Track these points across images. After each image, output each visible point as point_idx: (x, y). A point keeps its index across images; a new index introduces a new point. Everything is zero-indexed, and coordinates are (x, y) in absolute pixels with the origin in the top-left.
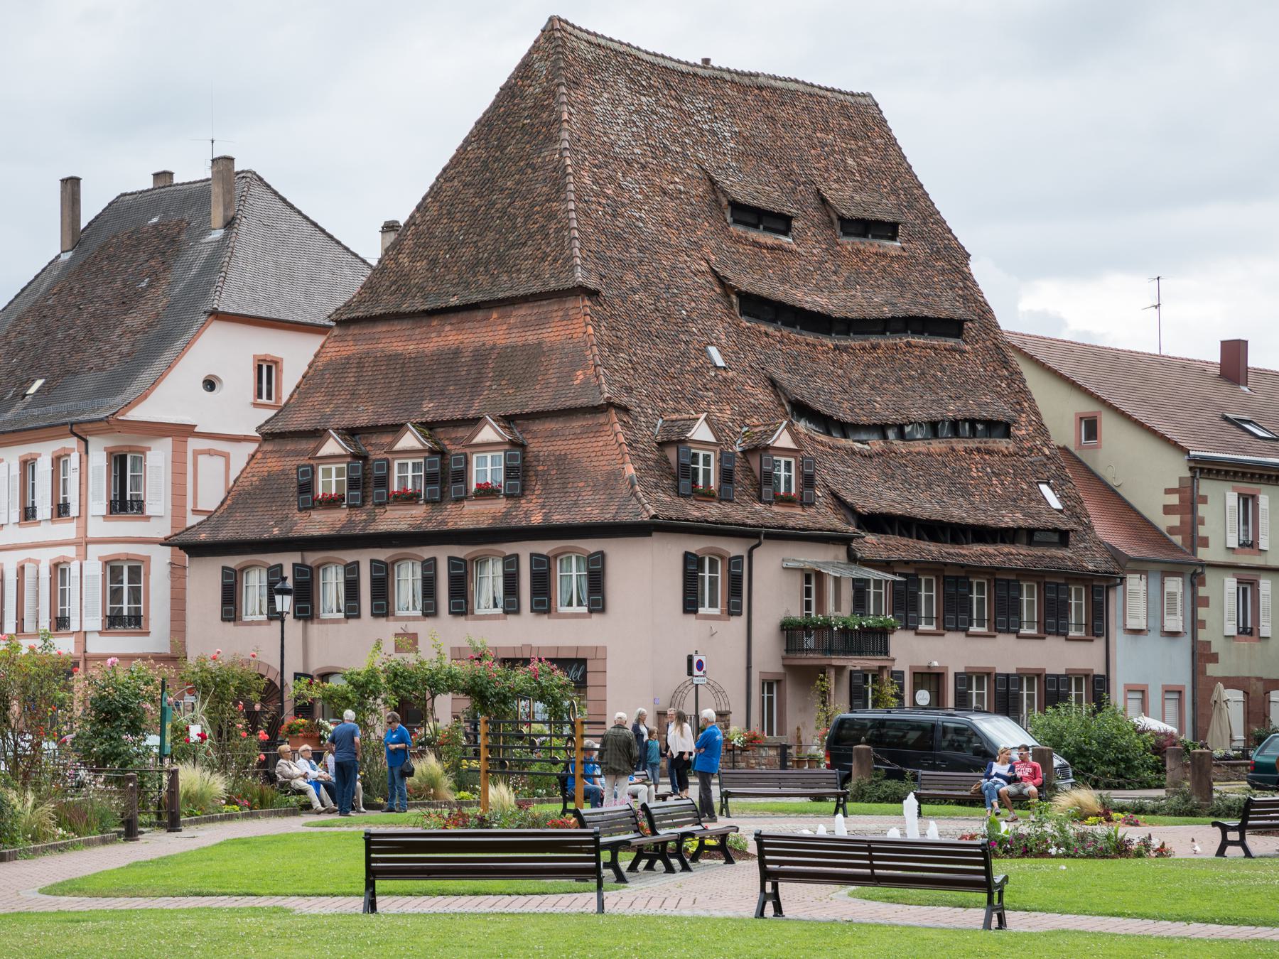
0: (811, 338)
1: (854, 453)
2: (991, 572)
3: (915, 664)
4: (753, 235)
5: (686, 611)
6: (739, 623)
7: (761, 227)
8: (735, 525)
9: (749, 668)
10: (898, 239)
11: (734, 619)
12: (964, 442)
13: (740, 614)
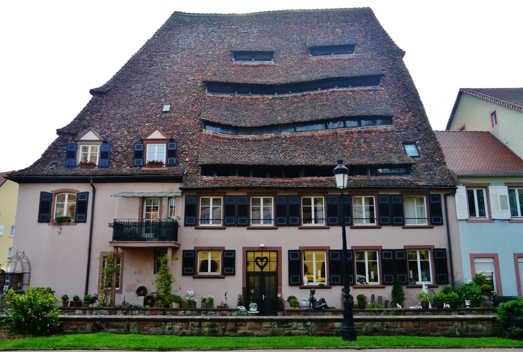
0: (258, 96)
1: (248, 140)
7: (253, 59)
9: (90, 250)
10: (354, 53)
11: (80, 225)
12: (347, 129)
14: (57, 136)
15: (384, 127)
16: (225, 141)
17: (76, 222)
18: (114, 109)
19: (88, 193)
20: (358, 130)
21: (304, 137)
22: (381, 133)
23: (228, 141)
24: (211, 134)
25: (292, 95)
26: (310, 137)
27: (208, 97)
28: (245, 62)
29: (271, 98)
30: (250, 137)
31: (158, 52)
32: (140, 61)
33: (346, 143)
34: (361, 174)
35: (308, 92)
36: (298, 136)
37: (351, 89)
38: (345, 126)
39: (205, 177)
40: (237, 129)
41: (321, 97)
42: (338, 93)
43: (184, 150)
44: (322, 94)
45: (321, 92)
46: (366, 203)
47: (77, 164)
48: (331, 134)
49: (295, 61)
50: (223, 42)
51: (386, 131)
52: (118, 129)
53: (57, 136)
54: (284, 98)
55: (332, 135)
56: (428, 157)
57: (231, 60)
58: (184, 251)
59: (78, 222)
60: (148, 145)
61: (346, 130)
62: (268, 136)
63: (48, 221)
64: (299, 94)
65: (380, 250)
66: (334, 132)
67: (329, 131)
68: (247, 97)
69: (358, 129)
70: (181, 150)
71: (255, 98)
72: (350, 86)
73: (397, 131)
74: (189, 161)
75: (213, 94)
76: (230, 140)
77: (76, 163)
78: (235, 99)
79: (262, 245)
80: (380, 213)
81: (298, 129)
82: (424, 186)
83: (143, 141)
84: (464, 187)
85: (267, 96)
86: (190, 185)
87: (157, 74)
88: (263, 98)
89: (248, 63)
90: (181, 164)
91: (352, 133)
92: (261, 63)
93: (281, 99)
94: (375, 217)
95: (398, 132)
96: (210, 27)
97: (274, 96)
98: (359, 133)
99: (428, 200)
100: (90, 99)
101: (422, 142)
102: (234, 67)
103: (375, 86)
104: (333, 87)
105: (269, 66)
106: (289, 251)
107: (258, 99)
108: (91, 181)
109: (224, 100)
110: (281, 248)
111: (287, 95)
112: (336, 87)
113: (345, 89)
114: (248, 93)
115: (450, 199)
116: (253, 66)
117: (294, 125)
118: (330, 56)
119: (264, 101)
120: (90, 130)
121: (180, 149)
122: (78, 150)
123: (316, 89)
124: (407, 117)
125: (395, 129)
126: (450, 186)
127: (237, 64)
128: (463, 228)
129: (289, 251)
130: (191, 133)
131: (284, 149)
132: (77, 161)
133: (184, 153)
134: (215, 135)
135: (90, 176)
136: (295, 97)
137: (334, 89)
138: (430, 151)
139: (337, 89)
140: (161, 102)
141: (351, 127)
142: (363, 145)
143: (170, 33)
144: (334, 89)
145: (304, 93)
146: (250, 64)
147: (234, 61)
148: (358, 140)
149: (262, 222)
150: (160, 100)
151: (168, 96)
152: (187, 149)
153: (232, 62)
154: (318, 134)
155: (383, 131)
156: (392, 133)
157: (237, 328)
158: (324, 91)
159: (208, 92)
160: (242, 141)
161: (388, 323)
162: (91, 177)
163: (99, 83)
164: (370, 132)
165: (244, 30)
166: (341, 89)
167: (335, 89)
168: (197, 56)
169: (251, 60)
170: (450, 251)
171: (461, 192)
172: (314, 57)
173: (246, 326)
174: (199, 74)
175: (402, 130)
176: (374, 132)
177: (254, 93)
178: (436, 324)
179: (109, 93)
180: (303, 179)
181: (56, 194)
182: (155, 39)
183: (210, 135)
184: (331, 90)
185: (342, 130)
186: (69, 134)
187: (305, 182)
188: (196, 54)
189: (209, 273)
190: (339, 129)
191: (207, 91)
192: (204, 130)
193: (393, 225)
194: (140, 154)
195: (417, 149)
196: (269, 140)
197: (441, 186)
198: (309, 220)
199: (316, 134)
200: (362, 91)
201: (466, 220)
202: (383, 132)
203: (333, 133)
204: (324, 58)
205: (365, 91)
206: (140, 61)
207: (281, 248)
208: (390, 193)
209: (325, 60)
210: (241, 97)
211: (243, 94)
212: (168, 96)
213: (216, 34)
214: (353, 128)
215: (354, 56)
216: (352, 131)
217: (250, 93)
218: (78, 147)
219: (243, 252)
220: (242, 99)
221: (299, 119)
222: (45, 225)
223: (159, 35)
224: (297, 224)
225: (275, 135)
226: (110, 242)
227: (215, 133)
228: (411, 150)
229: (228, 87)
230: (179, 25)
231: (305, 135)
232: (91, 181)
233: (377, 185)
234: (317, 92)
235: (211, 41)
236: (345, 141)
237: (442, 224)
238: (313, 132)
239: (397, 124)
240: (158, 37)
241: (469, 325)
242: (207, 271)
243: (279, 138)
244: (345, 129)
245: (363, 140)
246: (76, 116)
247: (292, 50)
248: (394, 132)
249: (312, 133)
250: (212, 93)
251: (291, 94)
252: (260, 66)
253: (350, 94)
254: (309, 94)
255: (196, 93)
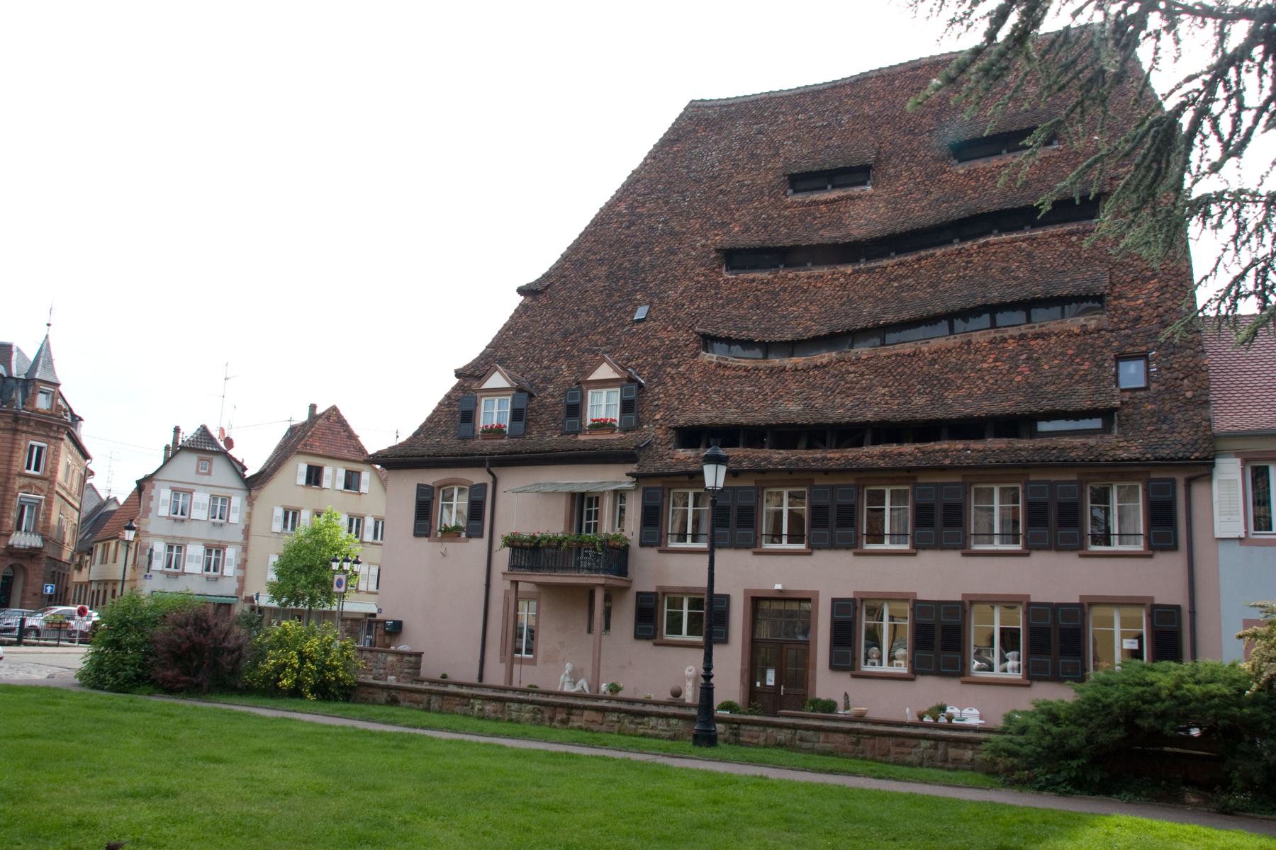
1: (784, 370)
2: (901, 473)
3: (755, 587)
4: (817, 196)
5: (417, 534)
6: (480, 545)
7: (829, 187)
8: (461, 456)
13: (481, 536)
14: (456, 381)
15: (1082, 320)
16: (740, 373)
17: (469, 536)
18: (552, 322)
19: (485, 485)
20: (1021, 332)
21: (897, 355)
22: (1071, 336)
23: (744, 374)
24: (714, 360)
25: (896, 260)
26: (909, 355)
27: (725, 280)
28: (812, 194)
29: (849, 272)
30: (789, 362)
31: (648, 194)
32: (612, 219)
33: (985, 365)
34: (998, 435)
35: (931, 251)
36: (885, 354)
37: (1028, 234)
38: (993, 325)
39: (681, 450)
40: (768, 348)
41: (957, 260)
42: (996, 246)
43: (656, 397)
44: (959, 252)
45: (960, 247)
46: (1002, 501)
47: (476, 433)
48: (958, 345)
49: (918, 180)
50: (777, 155)
51: (1085, 331)
52: (553, 362)
53: (456, 381)
54: (877, 270)
55: (959, 347)
56: (1167, 389)
57: (785, 193)
58: (638, 594)
59: (470, 537)
60: (590, 392)
61: (992, 335)
62: (824, 357)
63: (427, 534)
64: (909, 258)
65: (1025, 603)
66: (965, 340)
67: (955, 338)
68: (802, 273)
69: (1020, 329)
70: (651, 398)
71: (817, 274)
72: (1026, 228)
73: (1110, 328)
74: (661, 419)
75: (736, 274)
76: (749, 371)
77: (474, 430)
78: (776, 280)
79: (778, 587)
80: (1030, 522)
81: (891, 337)
82: (1130, 459)
83: (582, 386)
84: (1238, 461)
85: (842, 269)
86: (651, 467)
87: (639, 241)
88: (834, 273)
89: (817, 195)
90: (645, 426)
91: (1004, 340)
92: (845, 194)
93: (870, 271)
94: (1021, 532)
95: (1112, 331)
96: (756, 124)
97: (857, 267)
98: (1019, 340)
99: (1146, 490)
100: (516, 305)
101: (1163, 353)
102: (789, 207)
103: (1084, 222)
104: (989, 233)
105: (860, 198)
106: (834, 600)
107: (822, 277)
108: (487, 464)
109: (755, 284)
110: (817, 593)
111: (885, 262)
112: (995, 232)
113: (1014, 235)
114: (805, 265)
115: (1198, 490)
116: (826, 202)
117: (879, 331)
118: (999, 157)
119: (835, 280)
120: (497, 370)
121: (649, 395)
122: (478, 408)
123: (950, 242)
124: (1144, 292)
125: (1105, 324)
126: (1197, 459)
127: (795, 202)
128: (1228, 554)
129: (834, 600)
130: (675, 361)
131: (849, 385)
132: (476, 428)
133: (656, 403)
134: (722, 362)
135: (485, 454)
136: (901, 264)
137: (988, 239)
138: (1175, 375)
139: (996, 238)
140: (636, 299)
141: (1004, 327)
142: (1024, 368)
143: (675, 149)
144: (988, 239)
145: (923, 253)
146: (820, 199)
147: (791, 195)
148: (1013, 358)
149: (785, 540)
150: (634, 297)
151: (651, 285)
152: (661, 396)
153: (787, 197)
154: (930, 349)
155: (1077, 331)
156: (1096, 335)
157: (569, 718)
158: (966, 246)
159: (727, 270)
160: (772, 371)
161: (804, 733)
162: (487, 457)
163: (534, 272)
164: (1046, 334)
165: (823, 120)
166: (1004, 236)
167: (991, 239)
168: (721, 192)
169: (825, 188)
170: (1193, 612)
171: (1229, 472)
172: (961, 165)
173: (582, 715)
174: (716, 232)
175: (1123, 326)
176: (1056, 335)
177: (817, 263)
178: (889, 742)
179: (549, 290)
180: (866, 450)
181: (440, 488)
182: (646, 167)
183: (713, 362)
184: (982, 241)
185: (984, 334)
186: (472, 376)
187: (866, 457)
188: (720, 188)
189: (684, 636)
190: (978, 333)
191: (724, 268)
192: (703, 353)
193: (1059, 549)
194: (575, 410)
195: (1148, 368)
196: (825, 366)
197: (1172, 459)
198: (877, 537)
199: (925, 348)
200: (1052, 236)
201: (1240, 539)
202: (1076, 334)
203: (962, 343)
204: (981, 166)
205: (1059, 236)
206: (612, 219)
207: (817, 593)
208: (1053, 478)
209: (984, 169)
210: (790, 275)
211: (795, 269)
212: (651, 285)
213: (764, 139)
214: (1009, 329)
215: (1054, 150)
216: (1006, 335)
217: (809, 265)
218: (478, 402)
219: (745, 599)
220: (790, 280)
221: (890, 318)
222: (424, 540)
223: (654, 158)
224: (851, 544)
225: (839, 356)
226: (504, 574)
227: (722, 358)
228: (1132, 374)
229: (767, 257)
230: (697, 128)
231: (901, 351)
232: (487, 464)
233: (1020, 461)
234: (950, 249)
235: (752, 156)
236: (985, 361)
237: (1174, 548)
238: (919, 343)
239: (1113, 313)
240: (653, 161)
241: (950, 750)
242: (681, 634)
243: (844, 360)
244: (990, 333)
245: (1024, 357)
246: (489, 341)
247: (916, 153)
248: (1103, 332)
249: (917, 346)
250: (734, 271)
251: (893, 258)
252: (842, 200)
253: (1024, 245)
254: (932, 255)
255: (703, 275)
